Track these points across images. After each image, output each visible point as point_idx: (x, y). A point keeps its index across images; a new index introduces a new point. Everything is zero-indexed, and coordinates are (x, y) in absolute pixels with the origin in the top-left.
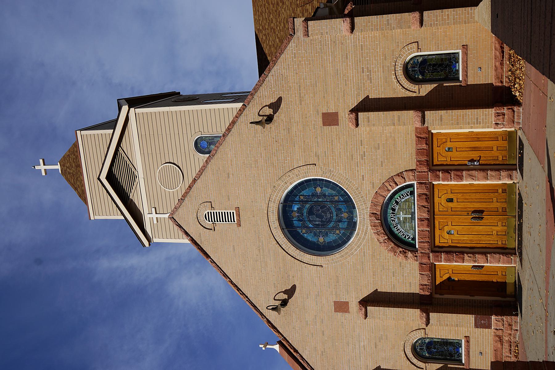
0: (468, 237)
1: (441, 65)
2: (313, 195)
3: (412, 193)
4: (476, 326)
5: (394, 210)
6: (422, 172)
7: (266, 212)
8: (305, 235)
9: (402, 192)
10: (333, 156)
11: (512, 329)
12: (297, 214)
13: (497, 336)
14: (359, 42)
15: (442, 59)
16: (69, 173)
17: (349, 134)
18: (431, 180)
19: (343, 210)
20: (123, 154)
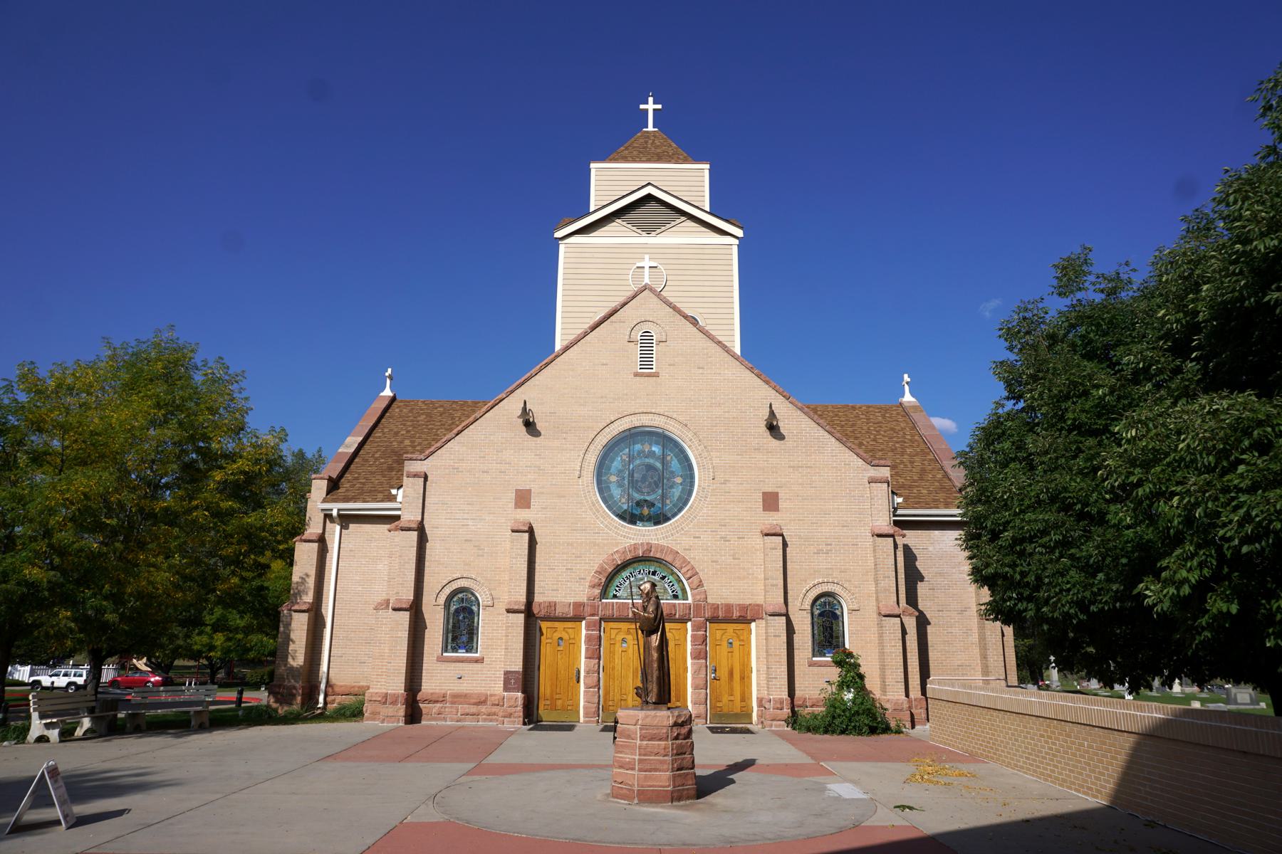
0: (618, 664)
1: (831, 636)
3: (676, 597)
4: (506, 673)
5: (654, 573)
6: (704, 610)
7: (653, 411)
8: (619, 459)
10: (725, 501)
11: (505, 717)
12: (647, 450)
13: (486, 698)
14: (860, 542)
15: (838, 637)
16: (646, 142)
17: (752, 523)
18: (695, 621)
19: (652, 509)
20: (678, 221)
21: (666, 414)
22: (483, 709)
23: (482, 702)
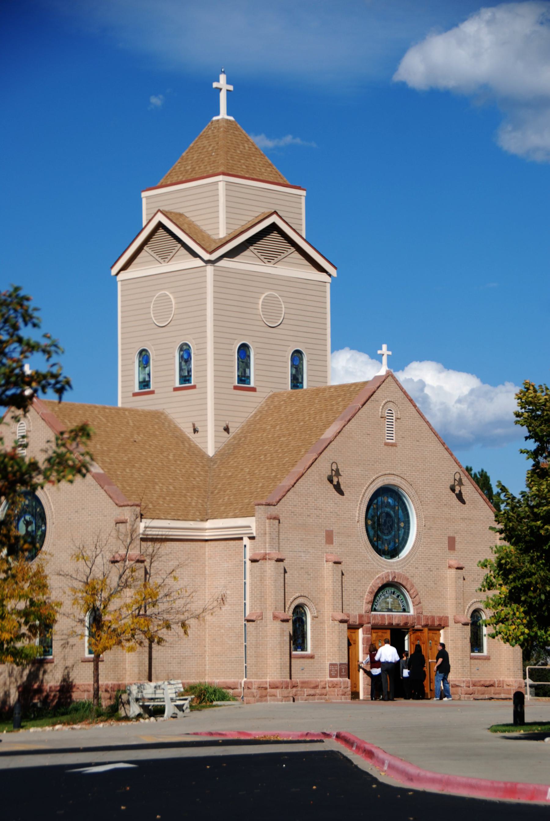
2: (399, 519)
3: (404, 610)
5: (394, 594)
7: (392, 472)
9: (405, 602)
12: (386, 501)
21: (401, 475)
22: (318, 691)
23: (316, 687)
